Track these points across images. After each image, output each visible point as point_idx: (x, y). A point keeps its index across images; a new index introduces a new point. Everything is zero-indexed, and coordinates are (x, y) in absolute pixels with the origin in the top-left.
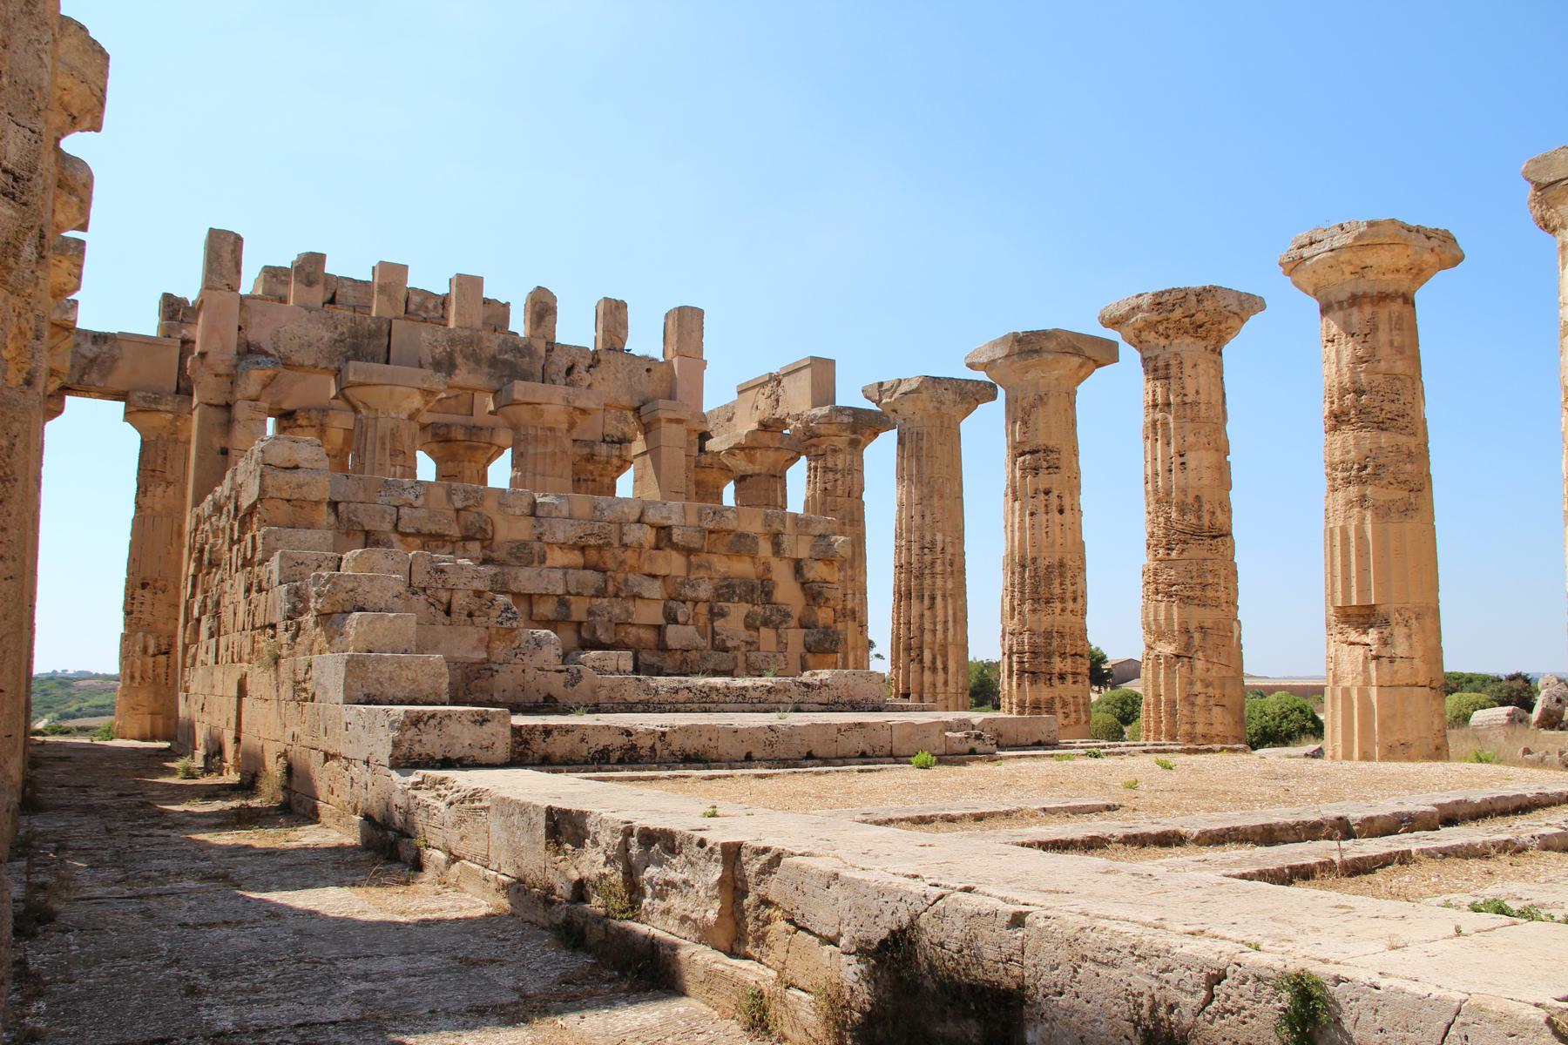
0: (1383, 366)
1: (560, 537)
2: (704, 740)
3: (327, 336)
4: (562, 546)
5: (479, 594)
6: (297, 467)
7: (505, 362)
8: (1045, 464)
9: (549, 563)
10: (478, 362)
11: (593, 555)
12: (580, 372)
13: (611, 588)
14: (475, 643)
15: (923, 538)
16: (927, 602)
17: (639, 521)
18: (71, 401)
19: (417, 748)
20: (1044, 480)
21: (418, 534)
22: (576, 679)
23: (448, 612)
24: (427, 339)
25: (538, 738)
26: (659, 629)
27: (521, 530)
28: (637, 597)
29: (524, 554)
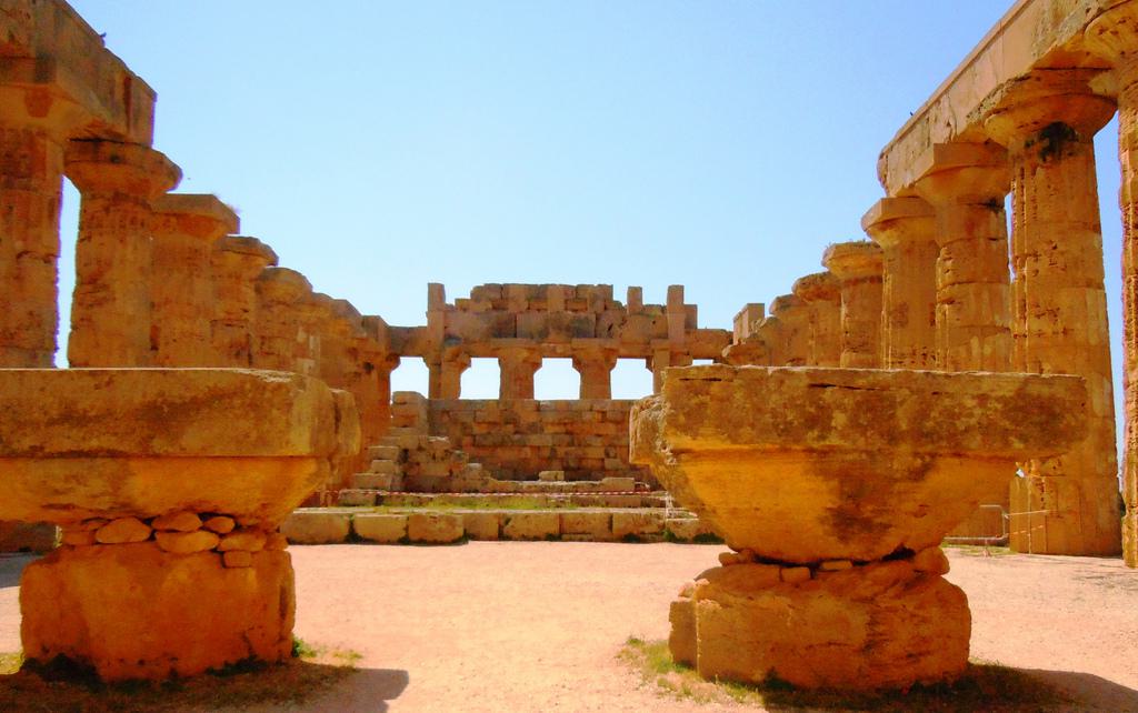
0: (856, 318)
1: (551, 420)
3: (485, 326)
4: (553, 424)
5: (446, 451)
6: (405, 403)
9: (546, 431)
10: (560, 329)
11: (569, 427)
12: (616, 328)
13: (576, 442)
17: (591, 410)
18: (402, 359)
21: (484, 422)
22: (486, 482)
24: (534, 321)
26: (603, 460)
27: (533, 418)
28: (589, 445)
29: (535, 428)
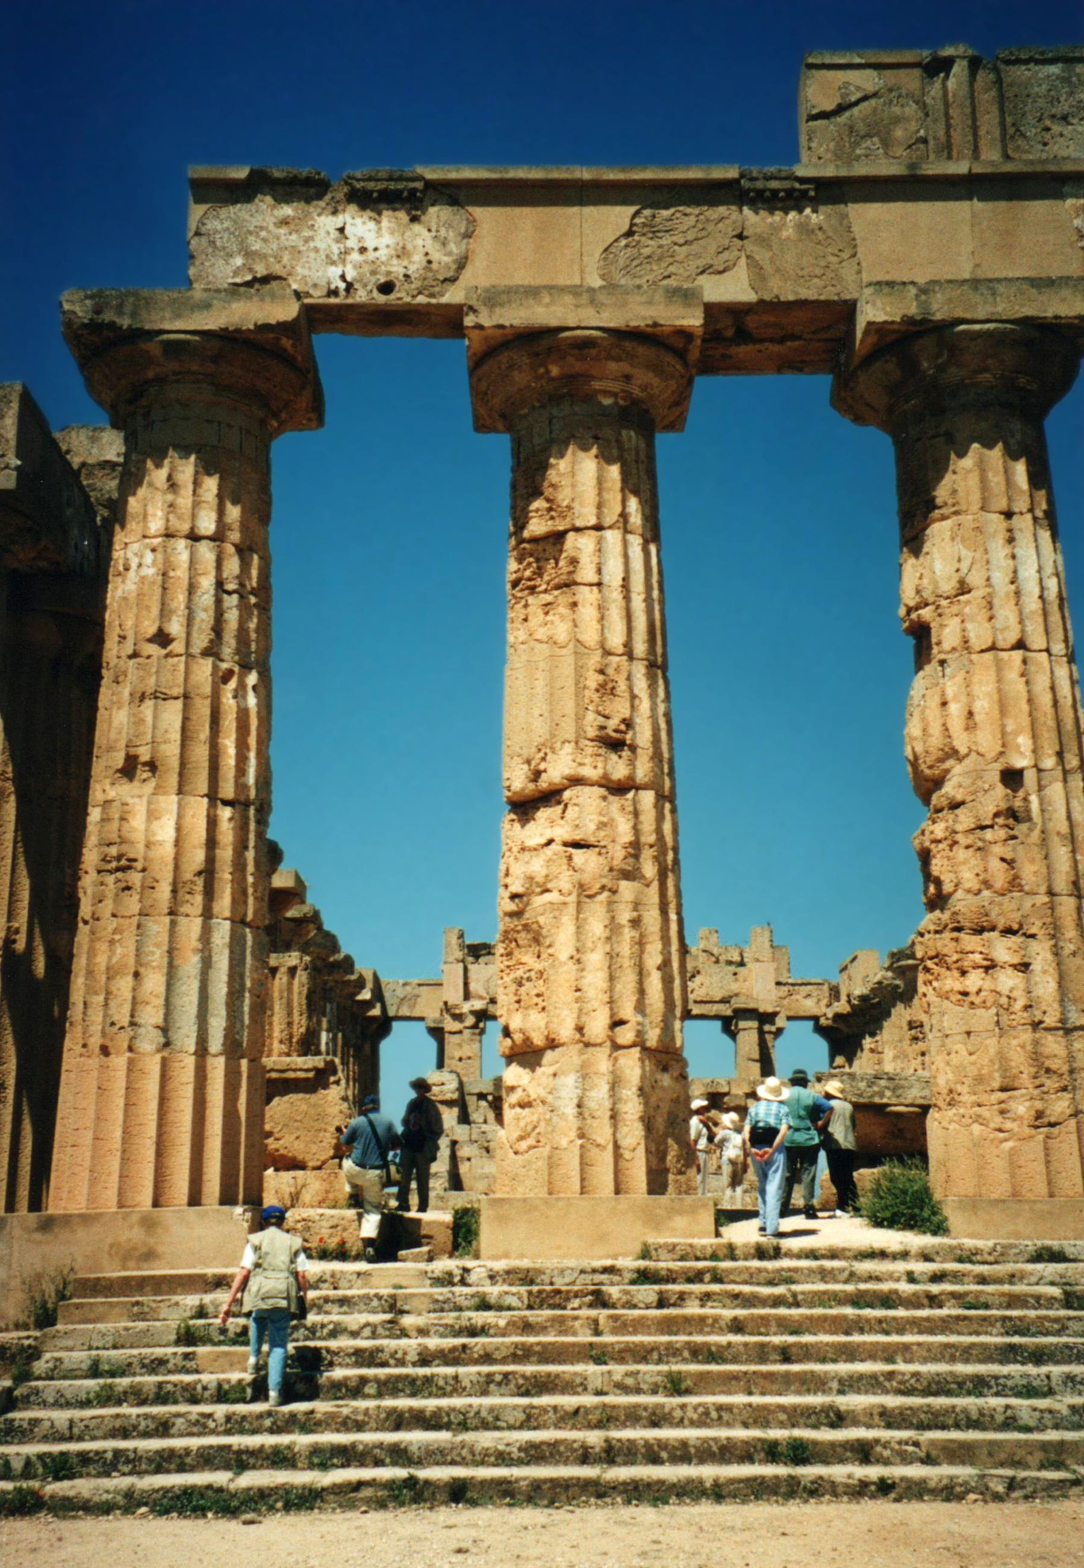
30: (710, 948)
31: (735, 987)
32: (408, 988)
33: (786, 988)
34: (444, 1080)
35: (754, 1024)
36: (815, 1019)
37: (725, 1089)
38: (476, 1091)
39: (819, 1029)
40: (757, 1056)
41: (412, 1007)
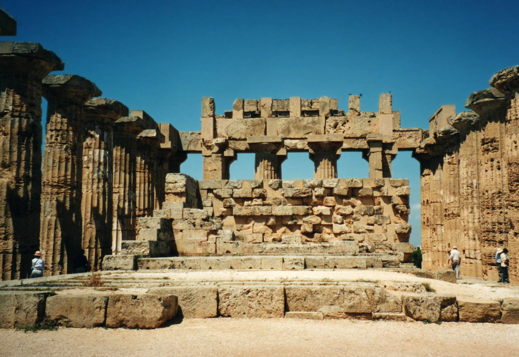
2: (196, 263)
6: (176, 182)
7: (310, 127)
8: (491, 148)
14: (203, 235)
15: (467, 182)
16: (470, 210)
19: (108, 265)
20: (491, 155)
23: (194, 226)
25: (145, 262)
30: (355, 107)
31: (368, 129)
32: (193, 135)
33: (398, 133)
34: (176, 180)
35: (380, 149)
36: (413, 149)
37: (360, 185)
38: (207, 187)
39: (415, 155)
40: (381, 168)
41: (195, 146)
